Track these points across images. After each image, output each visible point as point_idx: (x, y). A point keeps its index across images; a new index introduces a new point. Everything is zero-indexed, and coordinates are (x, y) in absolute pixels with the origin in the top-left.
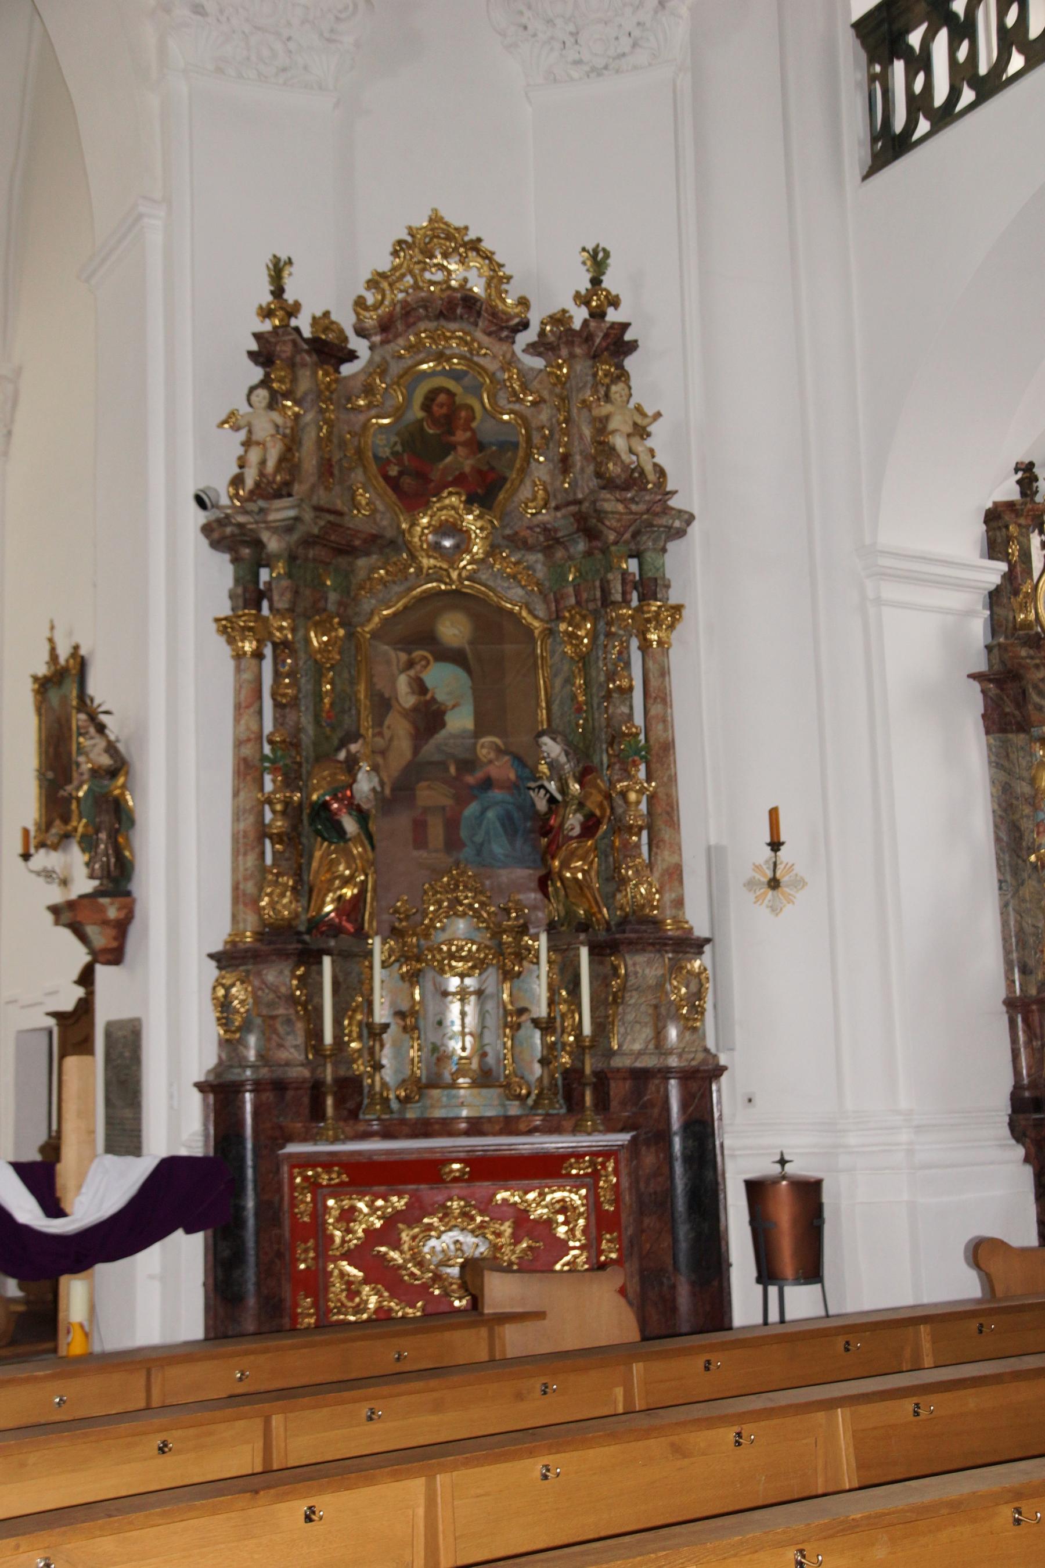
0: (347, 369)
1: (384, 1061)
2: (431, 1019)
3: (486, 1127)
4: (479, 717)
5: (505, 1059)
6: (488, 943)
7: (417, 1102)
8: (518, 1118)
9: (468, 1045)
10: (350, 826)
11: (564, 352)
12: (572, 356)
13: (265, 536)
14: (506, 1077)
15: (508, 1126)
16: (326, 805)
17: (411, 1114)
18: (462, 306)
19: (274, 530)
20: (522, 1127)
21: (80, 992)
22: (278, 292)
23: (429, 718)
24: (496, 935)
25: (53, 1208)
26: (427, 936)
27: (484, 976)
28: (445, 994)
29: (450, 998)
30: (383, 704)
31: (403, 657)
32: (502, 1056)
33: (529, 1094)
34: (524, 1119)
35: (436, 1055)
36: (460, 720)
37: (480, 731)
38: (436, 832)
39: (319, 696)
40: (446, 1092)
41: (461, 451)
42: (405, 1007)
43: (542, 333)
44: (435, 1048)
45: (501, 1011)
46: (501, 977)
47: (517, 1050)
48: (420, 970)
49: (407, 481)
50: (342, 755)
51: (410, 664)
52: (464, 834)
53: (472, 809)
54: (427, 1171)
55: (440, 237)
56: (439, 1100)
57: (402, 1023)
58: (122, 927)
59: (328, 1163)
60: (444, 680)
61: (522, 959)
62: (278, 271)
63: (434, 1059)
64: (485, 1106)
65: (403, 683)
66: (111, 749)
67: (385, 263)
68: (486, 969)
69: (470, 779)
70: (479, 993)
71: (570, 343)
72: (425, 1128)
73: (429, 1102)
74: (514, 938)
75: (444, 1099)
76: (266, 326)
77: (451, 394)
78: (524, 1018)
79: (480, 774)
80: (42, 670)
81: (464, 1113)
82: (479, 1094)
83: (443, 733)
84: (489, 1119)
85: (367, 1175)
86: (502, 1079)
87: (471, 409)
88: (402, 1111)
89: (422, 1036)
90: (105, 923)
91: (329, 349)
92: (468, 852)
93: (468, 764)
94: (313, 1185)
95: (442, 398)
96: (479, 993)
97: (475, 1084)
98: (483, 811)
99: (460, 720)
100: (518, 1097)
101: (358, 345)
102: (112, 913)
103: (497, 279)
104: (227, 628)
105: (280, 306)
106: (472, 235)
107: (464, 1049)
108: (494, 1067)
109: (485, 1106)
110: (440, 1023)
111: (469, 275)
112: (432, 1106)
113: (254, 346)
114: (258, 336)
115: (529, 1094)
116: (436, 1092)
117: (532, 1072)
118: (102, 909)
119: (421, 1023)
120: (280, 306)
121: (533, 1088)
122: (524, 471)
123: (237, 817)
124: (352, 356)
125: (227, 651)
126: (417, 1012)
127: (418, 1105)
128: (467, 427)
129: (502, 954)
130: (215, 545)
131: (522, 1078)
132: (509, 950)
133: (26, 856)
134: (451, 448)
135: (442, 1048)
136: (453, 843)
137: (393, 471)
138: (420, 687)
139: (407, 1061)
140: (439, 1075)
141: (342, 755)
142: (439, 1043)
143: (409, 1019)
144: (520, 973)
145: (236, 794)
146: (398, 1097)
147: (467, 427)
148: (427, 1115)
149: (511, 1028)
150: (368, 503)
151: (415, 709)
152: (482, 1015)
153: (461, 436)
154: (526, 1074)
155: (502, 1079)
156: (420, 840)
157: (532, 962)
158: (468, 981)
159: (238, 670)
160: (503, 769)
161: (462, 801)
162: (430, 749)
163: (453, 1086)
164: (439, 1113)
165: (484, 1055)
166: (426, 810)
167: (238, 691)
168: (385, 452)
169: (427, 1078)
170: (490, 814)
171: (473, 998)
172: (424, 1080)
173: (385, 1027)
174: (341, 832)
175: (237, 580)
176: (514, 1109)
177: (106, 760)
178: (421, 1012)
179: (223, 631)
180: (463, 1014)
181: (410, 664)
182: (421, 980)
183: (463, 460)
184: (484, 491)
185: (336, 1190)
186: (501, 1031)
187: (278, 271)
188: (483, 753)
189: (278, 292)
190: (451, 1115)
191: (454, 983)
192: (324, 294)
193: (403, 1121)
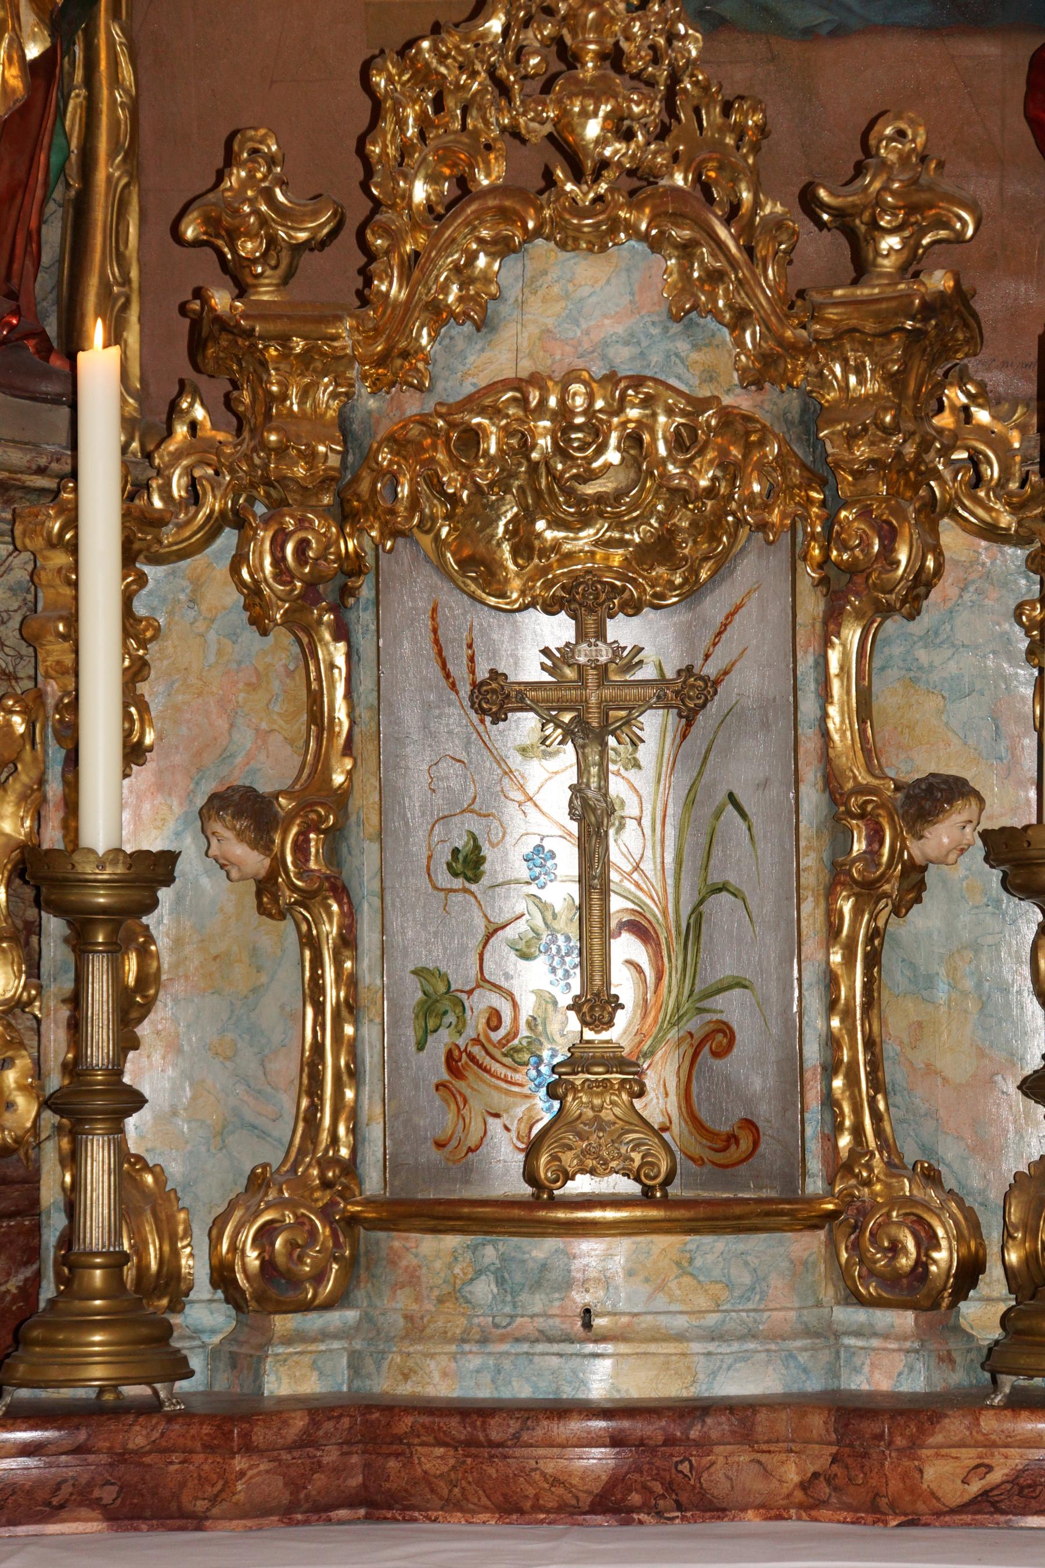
1: (148, 1071)
2: (425, 842)
3: (727, 1467)
5: (830, 1069)
6: (742, 401)
7: (328, 1306)
8: (918, 1414)
9: (623, 985)
14: (841, 1168)
17: (292, 1376)
20: (943, 1474)
26: (394, 364)
27: (714, 607)
28: (495, 698)
29: (525, 725)
32: (813, 1053)
33: (970, 1272)
34: (955, 1426)
35: (442, 1040)
40: (491, 1250)
42: (273, 771)
44: (439, 1002)
45: (812, 797)
46: (812, 606)
47: (897, 1019)
48: (353, 567)
56: (454, 1294)
57: (255, 862)
61: (932, 512)
63: (432, 1063)
64: (715, 1335)
68: (723, 564)
70: (688, 696)
73: (396, 1306)
74: (895, 381)
75: (484, 1289)
78: (943, 834)
81: (601, 1378)
82: (684, 1266)
84: (742, 1412)
86: (815, 1185)
88: (243, 1356)
89: (368, 936)
96: (688, 696)
97: (668, 1207)
100: (911, 1289)
107: (596, 1006)
108: (765, 1112)
109: (715, 1335)
110: (469, 864)
112: (415, 1329)
115: (970, 1272)
116: (435, 1250)
117: (986, 1148)
119: (364, 863)
121: (993, 1237)
126: (341, 799)
127: (335, 1318)
129: (821, 473)
131: (932, 1177)
132: (862, 451)
135: (482, 1001)
139: (287, 1068)
140: (462, 1154)
142: (461, 976)
143: (299, 839)
144: (921, 584)
146: (222, 1276)
148: (384, 1384)
149: (867, 892)
152: (706, 815)
154: (952, 1156)
155: (815, 1185)
157: (991, 533)
158: (622, 630)
163: (539, 1211)
164: (448, 1376)
165: (718, 1039)
169: (391, 1165)
171: (652, 725)
172: (373, 1182)
173: (154, 870)
176: (886, 1360)
178: (365, 804)
180: (593, 818)
182: (362, 618)
186: (812, 911)
190: (521, 1389)
191: (534, 641)
193: (236, 1422)
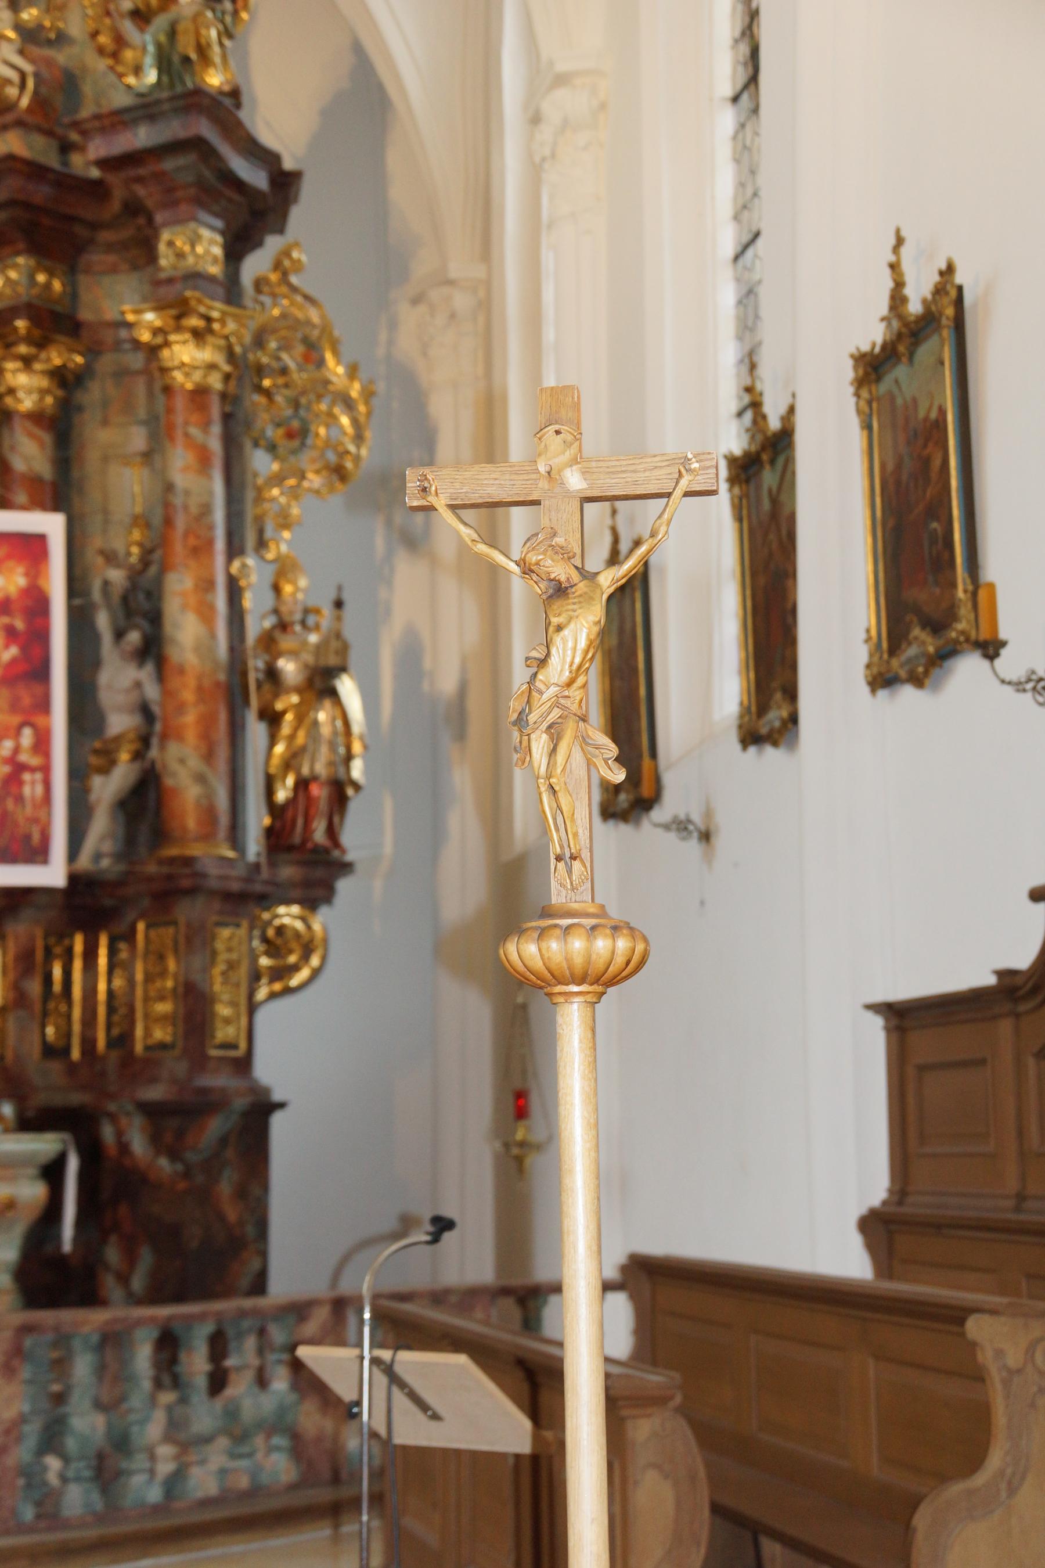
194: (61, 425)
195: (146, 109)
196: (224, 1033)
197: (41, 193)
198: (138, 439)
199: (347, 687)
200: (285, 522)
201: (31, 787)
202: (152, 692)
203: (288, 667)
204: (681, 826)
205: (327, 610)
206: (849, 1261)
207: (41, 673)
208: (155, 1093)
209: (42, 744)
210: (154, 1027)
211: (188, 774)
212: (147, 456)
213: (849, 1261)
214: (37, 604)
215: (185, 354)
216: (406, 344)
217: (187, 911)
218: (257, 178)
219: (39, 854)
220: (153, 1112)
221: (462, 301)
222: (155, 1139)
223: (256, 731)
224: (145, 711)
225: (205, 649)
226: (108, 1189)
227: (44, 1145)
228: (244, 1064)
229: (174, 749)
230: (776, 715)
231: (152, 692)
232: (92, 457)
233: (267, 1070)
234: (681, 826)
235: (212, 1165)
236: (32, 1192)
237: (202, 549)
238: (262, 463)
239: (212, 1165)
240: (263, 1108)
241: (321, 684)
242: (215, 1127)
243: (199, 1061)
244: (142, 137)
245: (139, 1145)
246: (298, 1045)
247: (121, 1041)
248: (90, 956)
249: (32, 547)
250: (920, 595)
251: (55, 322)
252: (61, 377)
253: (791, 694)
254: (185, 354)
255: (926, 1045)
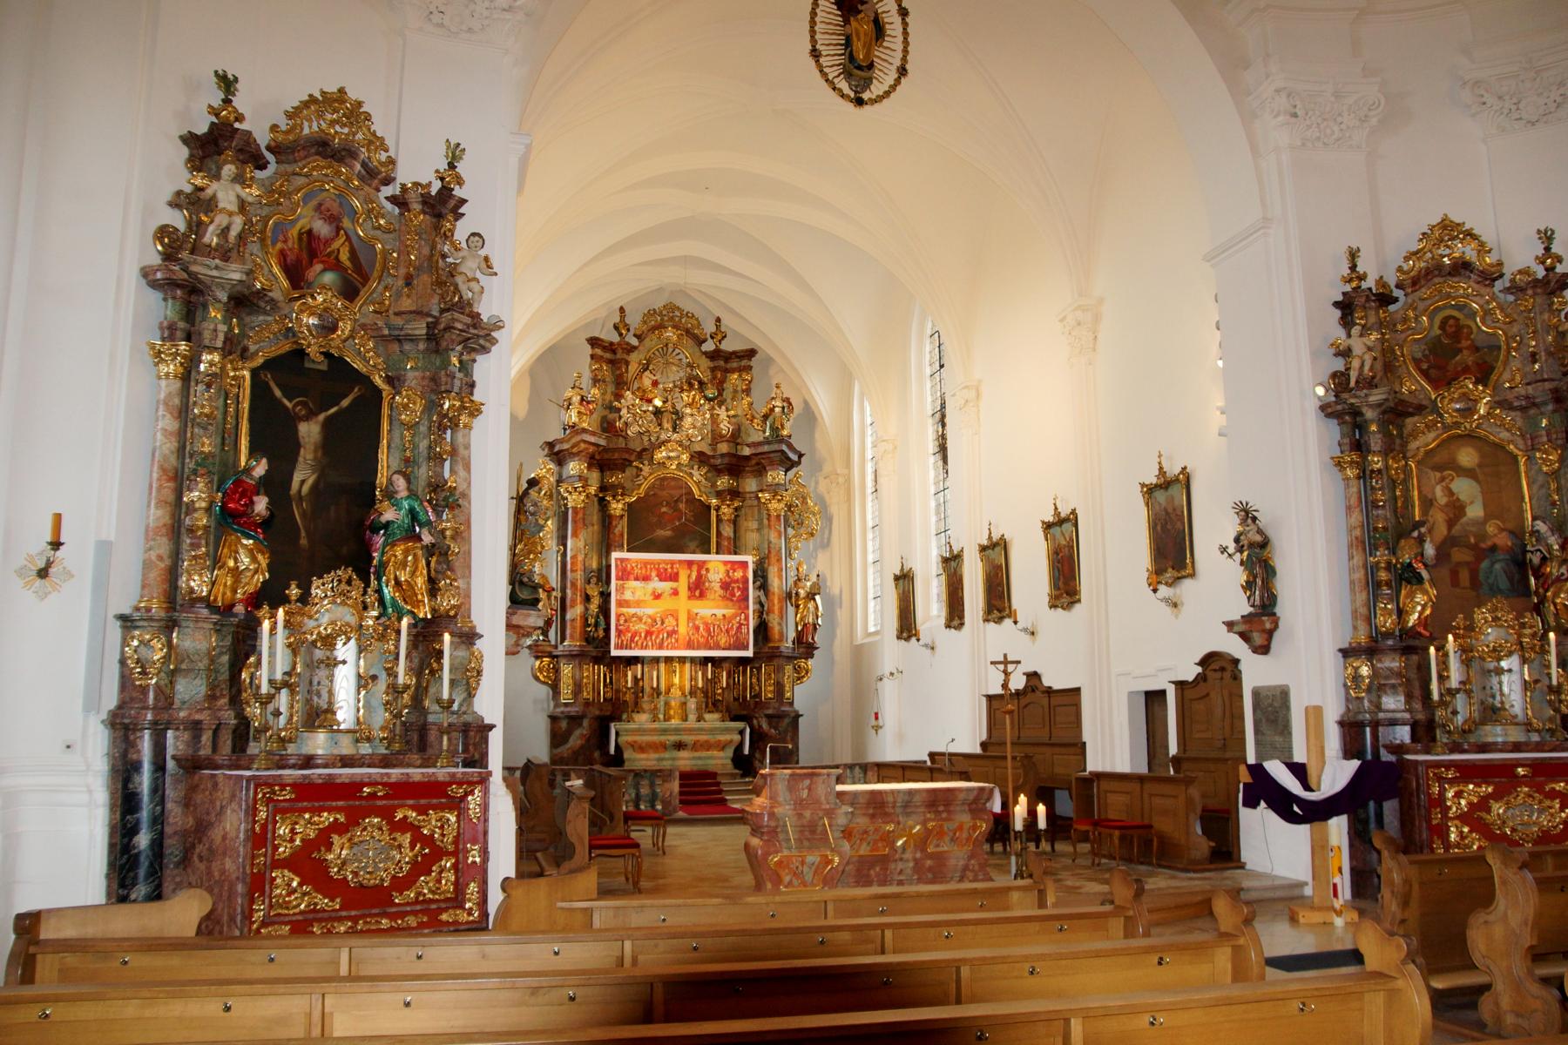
0: (1392, 308)
4: (1485, 506)
10: (1425, 574)
11: (1530, 292)
12: (1535, 294)
13: (1364, 410)
15: (1538, 747)
16: (1410, 565)
18: (1462, 267)
19: (1371, 406)
21: (1199, 669)
22: (1353, 268)
23: (1456, 509)
24: (1520, 635)
25: (1307, 788)
30: (1428, 503)
31: (1438, 475)
36: (1475, 511)
37: (1488, 516)
38: (1464, 576)
39: (1395, 499)
41: (1465, 352)
43: (1512, 281)
49: (1433, 372)
50: (1415, 534)
51: (1443, 479)
52: (1481, 577)
53: (1485, 564)
54: (1507, 769)
55: (1448, 230)
58: (1270, 634)
59: (1449, 765)
60: (1464, 488)
62: (1353, 255)
65: (1439, 491)
66: (1260, 531)
67: (1415, 247)
69: (1483, 546)
71: (1534, 287)
72: (1484, 748)
76: (1348, 288)
77: (1457, 320)
79: (1489, 543)
80: (1152, 479)
83: (1464, 520)
85: (1468, 772)
87: (1469, 327)
90: (1264, 631)
91: (1385, 299)
92: (1485, 587)
93: (1483, 536)
94: (1440, 779)
95: (1451, 322)
98: (1493, 564)
99: (1475, 511)
101: (1397, 293)
102: (1268, 626)
103: (1483, 249)
104: (1339, 464)
105: (1355, 275)
106: (1467, 227)
111: (1468, 251)
113: (1340, 298)
114: (1344, 294)
118: (1263, 623)
120: (1355, 275)
122: (1506, 363)
123: (1352, 570)
124: (1396, 300)
125: (1339, 476)
128: (1468, 338)
130: (1328, 416)
133: (1155, 591)
134: (1460, 350)
136: (1475, 583)
137: (1425, 366)
138: (1451, 493)
141: (1415, 534)
145: (1351, 558)
147: (1468, 338)
150: (1413, 385)
151: (1447, 505)
153: (1465, 343)
156: (1455, 581)
159: (1347, 487)
160: (1504, 540)
161: (1479, 560)
162: (1457, 529)
166: (1459, 564)
167: (1348, 498)
168: (1419, 355)
170: (1498, 566)
174: (1420, 580)
175: (1343, 435)
177: (1258, 538)
179: (1338, 464)
181: (1443, 479)
183: (1467, 357)
184: (1484, 374)
185: (1452, 782)
187: (1353, 255)
188: (1490, 529)
189: (1353, 268)
192: (1378, 268)
194: (735, 522)
195: (767, 442)
196: (788, 695)
197: (734, 461)
198: (754, 525)
199: (817, 598)
200: (797, 548)
201: (744, 630)
202: (763, 599)
203: (802, 593)
204: (926, 646)
205: (814, 578)
206: (978, 750)
207: (746, 598)
208: (770, 712)
209: (747, 618)
210: (768, 692)
211: (773, 620)
212: (758, 530)
213: (978, 750)
214: (746, 581)
215: (774, 505)
216: (822, 488)
217: (775, 662)
218: (794, 457)
219: (746, 648)
220: (768, 716)
221: (841, 480)
222: (770, 724)
223: (791, 610)
224: (762, 605)
225: (780, 588)
226: (758, 739)
227: (740, 725)
228: (791, 704)
229: (771, 617)
230: (956, 622)
231: (763, 599)
232: (742, 531)
233: (797, 706)
234: (926, 646)
235: (786, 731)
236: (737, 738)
237: (779, 560)
238: (791, 532)
239: (786, 731)
240: (798, 716)
241: (811, 596)
242: (786, 721)
243: (782, 703)
244: (766, 448)
245: (765, 726)
246: (802, 696)
247: (759, 695)
248: (744, 672)
249: (744, 565)
250: (997, 603)
251: (734, 493)
252: (736, 509)
253: (961, 617)
254: (774, 505)
255: (995, 704)
